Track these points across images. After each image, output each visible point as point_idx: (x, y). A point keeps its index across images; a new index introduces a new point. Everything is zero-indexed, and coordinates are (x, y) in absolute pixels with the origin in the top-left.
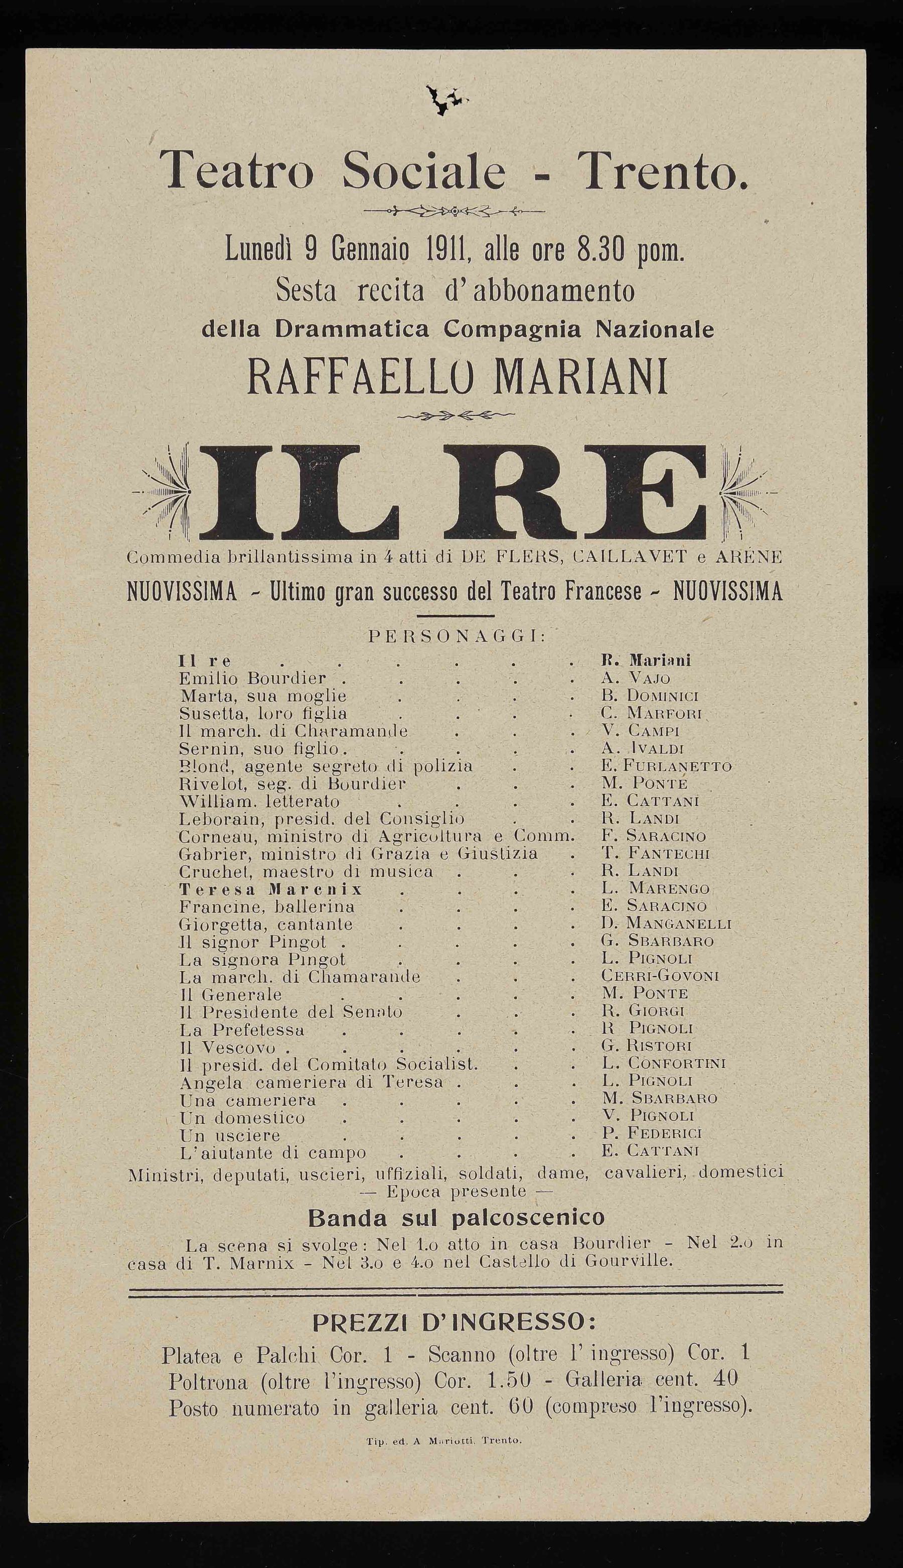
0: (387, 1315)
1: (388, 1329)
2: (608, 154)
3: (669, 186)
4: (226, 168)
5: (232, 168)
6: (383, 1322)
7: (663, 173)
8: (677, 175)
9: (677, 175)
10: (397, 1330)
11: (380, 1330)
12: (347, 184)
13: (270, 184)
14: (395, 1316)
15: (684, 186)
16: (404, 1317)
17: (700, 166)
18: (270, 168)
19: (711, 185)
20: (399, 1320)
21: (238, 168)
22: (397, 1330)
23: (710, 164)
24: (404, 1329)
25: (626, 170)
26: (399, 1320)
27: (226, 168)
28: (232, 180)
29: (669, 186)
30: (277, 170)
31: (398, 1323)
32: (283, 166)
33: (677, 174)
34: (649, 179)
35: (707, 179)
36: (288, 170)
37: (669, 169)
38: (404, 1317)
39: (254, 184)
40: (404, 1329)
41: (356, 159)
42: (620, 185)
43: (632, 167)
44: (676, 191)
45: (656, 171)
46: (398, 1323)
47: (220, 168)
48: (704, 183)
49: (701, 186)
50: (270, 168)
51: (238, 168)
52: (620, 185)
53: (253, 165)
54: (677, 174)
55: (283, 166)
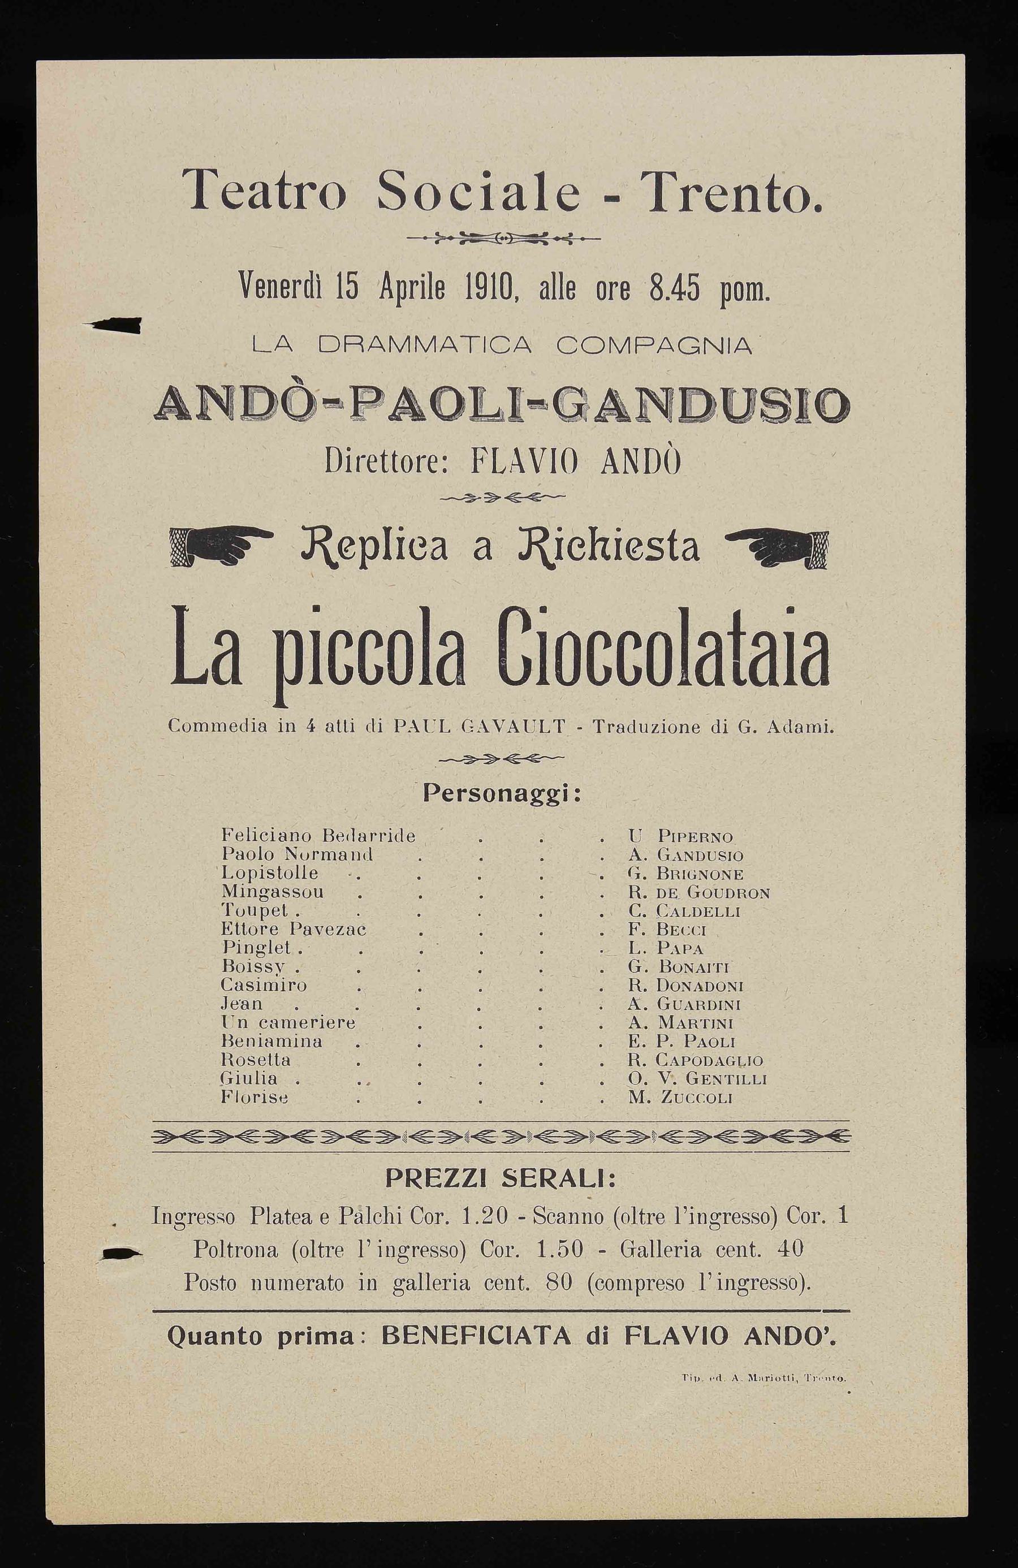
0: (465, 1170)
1: (465, 1185)
2: (674, 174)
3: (738, 208)
4: (252, 188)
5: (259, 188)
6: (461, 1178)
7: (732, 195)
8: (747, 198)
9: (747, 198)
10: (475, 1185)
11: (457, 1185)
12: (382, 205)
13: (300, 205)
14: (474, 1171)
15: (755, 208)
16: (483, 1171)
17: (771, 187)
18: (300, 188)
19: (784, 208)
20: (477, 1176)
21: (265, 187)
22: (475, 1185)
23: (783, 184)
24: (483, 1185)
25: (693, 192)
26: (477, 1176)
27: (252, 188)
28: (259, 200)
29: (738, 208)
30: (307, 189)
31: (477, 1178)
32: (313, 186)
33: (747, 196)
34: (717, 201)
35: (779, 202)
36: (319, 189)
37: (738, 191)
38: (483, 1171)
39: (283, 205)
40: (483, 1185)
41: (392, 179)
42: (686, 207)
43: (699, 189)
44: (746, 215)
45: (724, 193)
46: (477, 1178)
47: (246, 188)
48: (776, 206)
49: (772, 208)
50: (300, 188)
51: (265, 187)
52: (686, 207)
53: (282, 184)
54: (747, 196)
55: (313, 186)
